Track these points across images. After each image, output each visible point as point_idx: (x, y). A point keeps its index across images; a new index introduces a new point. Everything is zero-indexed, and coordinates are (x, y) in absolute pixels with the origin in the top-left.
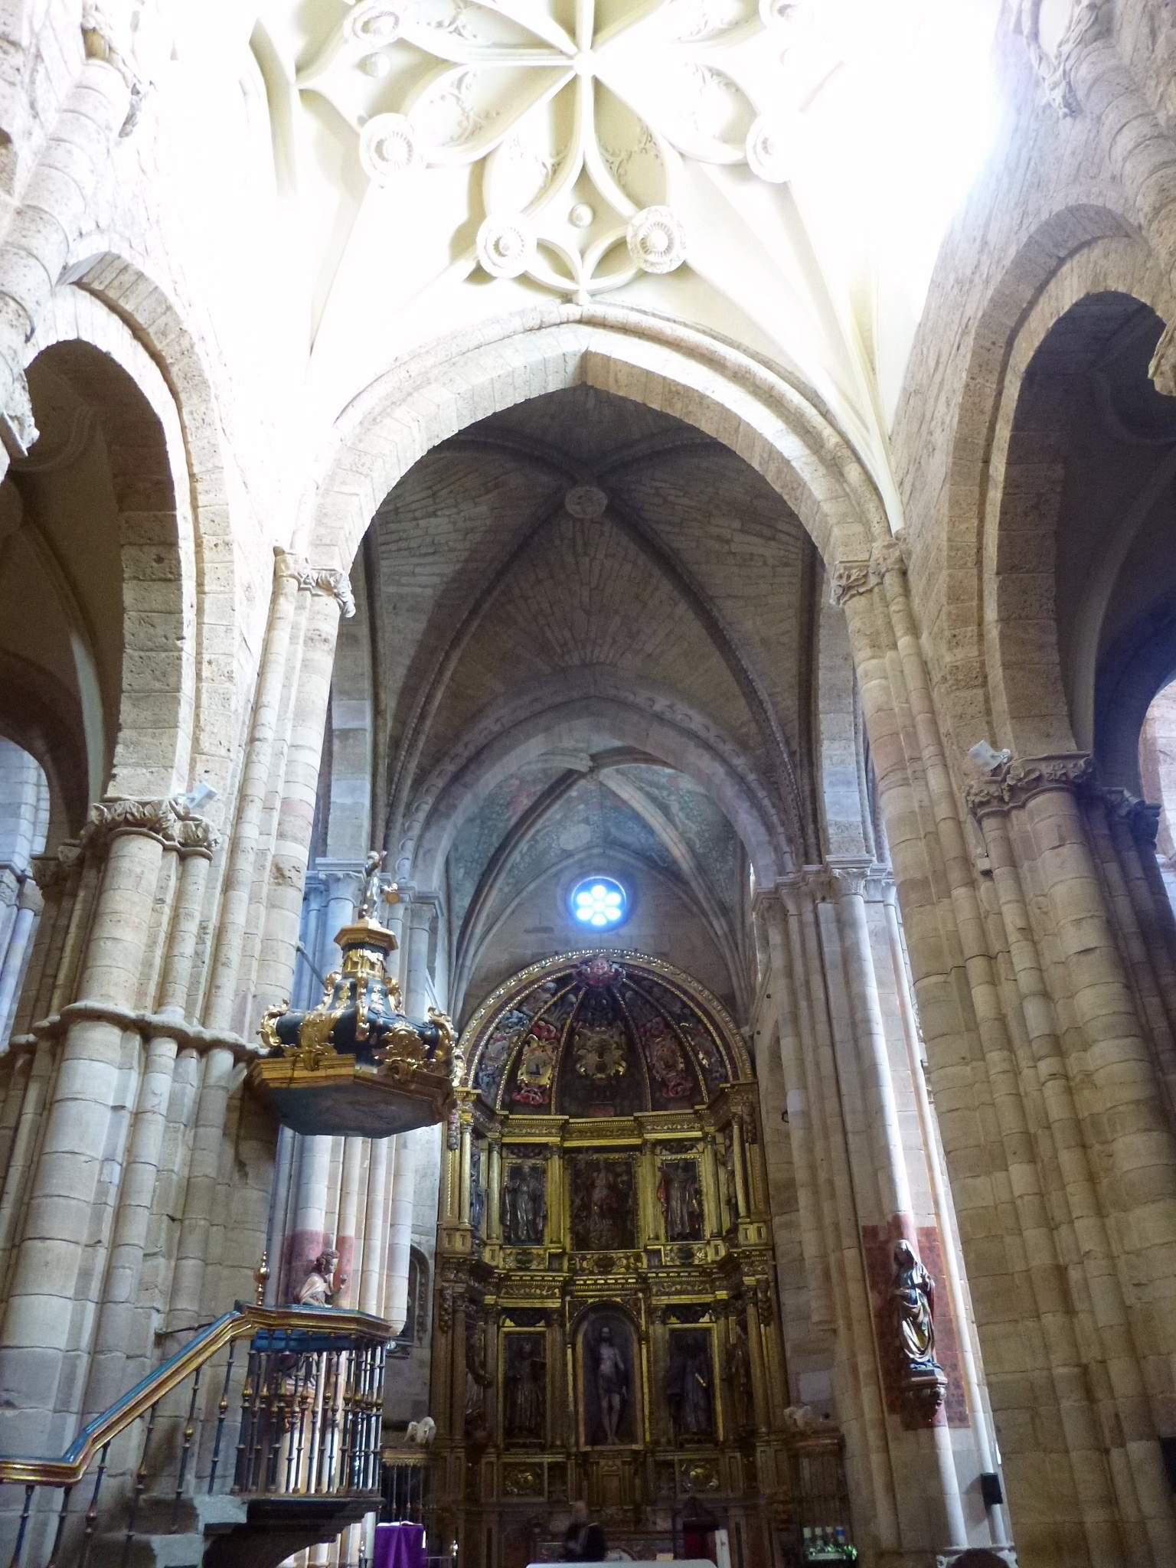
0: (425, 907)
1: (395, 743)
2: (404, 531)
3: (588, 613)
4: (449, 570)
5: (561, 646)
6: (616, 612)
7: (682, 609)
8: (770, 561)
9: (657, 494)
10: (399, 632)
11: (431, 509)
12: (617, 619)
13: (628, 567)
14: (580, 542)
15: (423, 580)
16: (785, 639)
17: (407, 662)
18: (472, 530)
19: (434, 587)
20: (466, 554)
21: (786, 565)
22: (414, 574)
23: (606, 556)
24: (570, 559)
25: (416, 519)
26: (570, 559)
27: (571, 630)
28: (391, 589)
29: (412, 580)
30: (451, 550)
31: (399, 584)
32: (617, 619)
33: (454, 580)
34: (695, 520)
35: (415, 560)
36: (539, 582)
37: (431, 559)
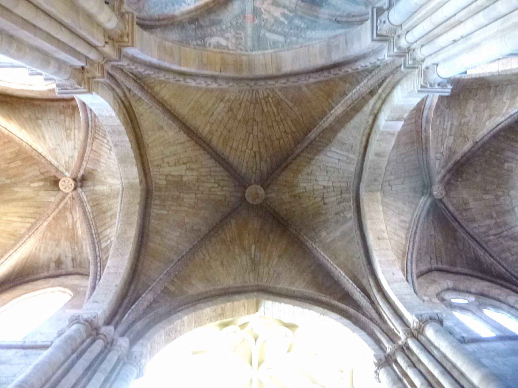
0: (384, 33)
1: (372, 93)
2: (339, 182)
3: (254, 120)
4: (321, 157)
5: (269, 102)
6: (240, 121)
7: (204, 130)
8: (166, 165)
10: (353, 136)
11: (325, 191)
12: (239, 117)
13: (234, 146)
14: (258, 159)
15: (336, 156)
16: (150, 133)
17: (352, 121)
19: (330, 150)
20: (313, 162)
21: (157, 166)
22: (339, 160)
23: (245, 151)
24: (263, 150)
25: (334, 187)
26: (263, 150)
28: (351, 156)
29: (341, 158)
31: (347, 157)
32: (239, 117)
34: (203, 176)
35: (338, 167)
36: (279, 140)
37: (330, 165)
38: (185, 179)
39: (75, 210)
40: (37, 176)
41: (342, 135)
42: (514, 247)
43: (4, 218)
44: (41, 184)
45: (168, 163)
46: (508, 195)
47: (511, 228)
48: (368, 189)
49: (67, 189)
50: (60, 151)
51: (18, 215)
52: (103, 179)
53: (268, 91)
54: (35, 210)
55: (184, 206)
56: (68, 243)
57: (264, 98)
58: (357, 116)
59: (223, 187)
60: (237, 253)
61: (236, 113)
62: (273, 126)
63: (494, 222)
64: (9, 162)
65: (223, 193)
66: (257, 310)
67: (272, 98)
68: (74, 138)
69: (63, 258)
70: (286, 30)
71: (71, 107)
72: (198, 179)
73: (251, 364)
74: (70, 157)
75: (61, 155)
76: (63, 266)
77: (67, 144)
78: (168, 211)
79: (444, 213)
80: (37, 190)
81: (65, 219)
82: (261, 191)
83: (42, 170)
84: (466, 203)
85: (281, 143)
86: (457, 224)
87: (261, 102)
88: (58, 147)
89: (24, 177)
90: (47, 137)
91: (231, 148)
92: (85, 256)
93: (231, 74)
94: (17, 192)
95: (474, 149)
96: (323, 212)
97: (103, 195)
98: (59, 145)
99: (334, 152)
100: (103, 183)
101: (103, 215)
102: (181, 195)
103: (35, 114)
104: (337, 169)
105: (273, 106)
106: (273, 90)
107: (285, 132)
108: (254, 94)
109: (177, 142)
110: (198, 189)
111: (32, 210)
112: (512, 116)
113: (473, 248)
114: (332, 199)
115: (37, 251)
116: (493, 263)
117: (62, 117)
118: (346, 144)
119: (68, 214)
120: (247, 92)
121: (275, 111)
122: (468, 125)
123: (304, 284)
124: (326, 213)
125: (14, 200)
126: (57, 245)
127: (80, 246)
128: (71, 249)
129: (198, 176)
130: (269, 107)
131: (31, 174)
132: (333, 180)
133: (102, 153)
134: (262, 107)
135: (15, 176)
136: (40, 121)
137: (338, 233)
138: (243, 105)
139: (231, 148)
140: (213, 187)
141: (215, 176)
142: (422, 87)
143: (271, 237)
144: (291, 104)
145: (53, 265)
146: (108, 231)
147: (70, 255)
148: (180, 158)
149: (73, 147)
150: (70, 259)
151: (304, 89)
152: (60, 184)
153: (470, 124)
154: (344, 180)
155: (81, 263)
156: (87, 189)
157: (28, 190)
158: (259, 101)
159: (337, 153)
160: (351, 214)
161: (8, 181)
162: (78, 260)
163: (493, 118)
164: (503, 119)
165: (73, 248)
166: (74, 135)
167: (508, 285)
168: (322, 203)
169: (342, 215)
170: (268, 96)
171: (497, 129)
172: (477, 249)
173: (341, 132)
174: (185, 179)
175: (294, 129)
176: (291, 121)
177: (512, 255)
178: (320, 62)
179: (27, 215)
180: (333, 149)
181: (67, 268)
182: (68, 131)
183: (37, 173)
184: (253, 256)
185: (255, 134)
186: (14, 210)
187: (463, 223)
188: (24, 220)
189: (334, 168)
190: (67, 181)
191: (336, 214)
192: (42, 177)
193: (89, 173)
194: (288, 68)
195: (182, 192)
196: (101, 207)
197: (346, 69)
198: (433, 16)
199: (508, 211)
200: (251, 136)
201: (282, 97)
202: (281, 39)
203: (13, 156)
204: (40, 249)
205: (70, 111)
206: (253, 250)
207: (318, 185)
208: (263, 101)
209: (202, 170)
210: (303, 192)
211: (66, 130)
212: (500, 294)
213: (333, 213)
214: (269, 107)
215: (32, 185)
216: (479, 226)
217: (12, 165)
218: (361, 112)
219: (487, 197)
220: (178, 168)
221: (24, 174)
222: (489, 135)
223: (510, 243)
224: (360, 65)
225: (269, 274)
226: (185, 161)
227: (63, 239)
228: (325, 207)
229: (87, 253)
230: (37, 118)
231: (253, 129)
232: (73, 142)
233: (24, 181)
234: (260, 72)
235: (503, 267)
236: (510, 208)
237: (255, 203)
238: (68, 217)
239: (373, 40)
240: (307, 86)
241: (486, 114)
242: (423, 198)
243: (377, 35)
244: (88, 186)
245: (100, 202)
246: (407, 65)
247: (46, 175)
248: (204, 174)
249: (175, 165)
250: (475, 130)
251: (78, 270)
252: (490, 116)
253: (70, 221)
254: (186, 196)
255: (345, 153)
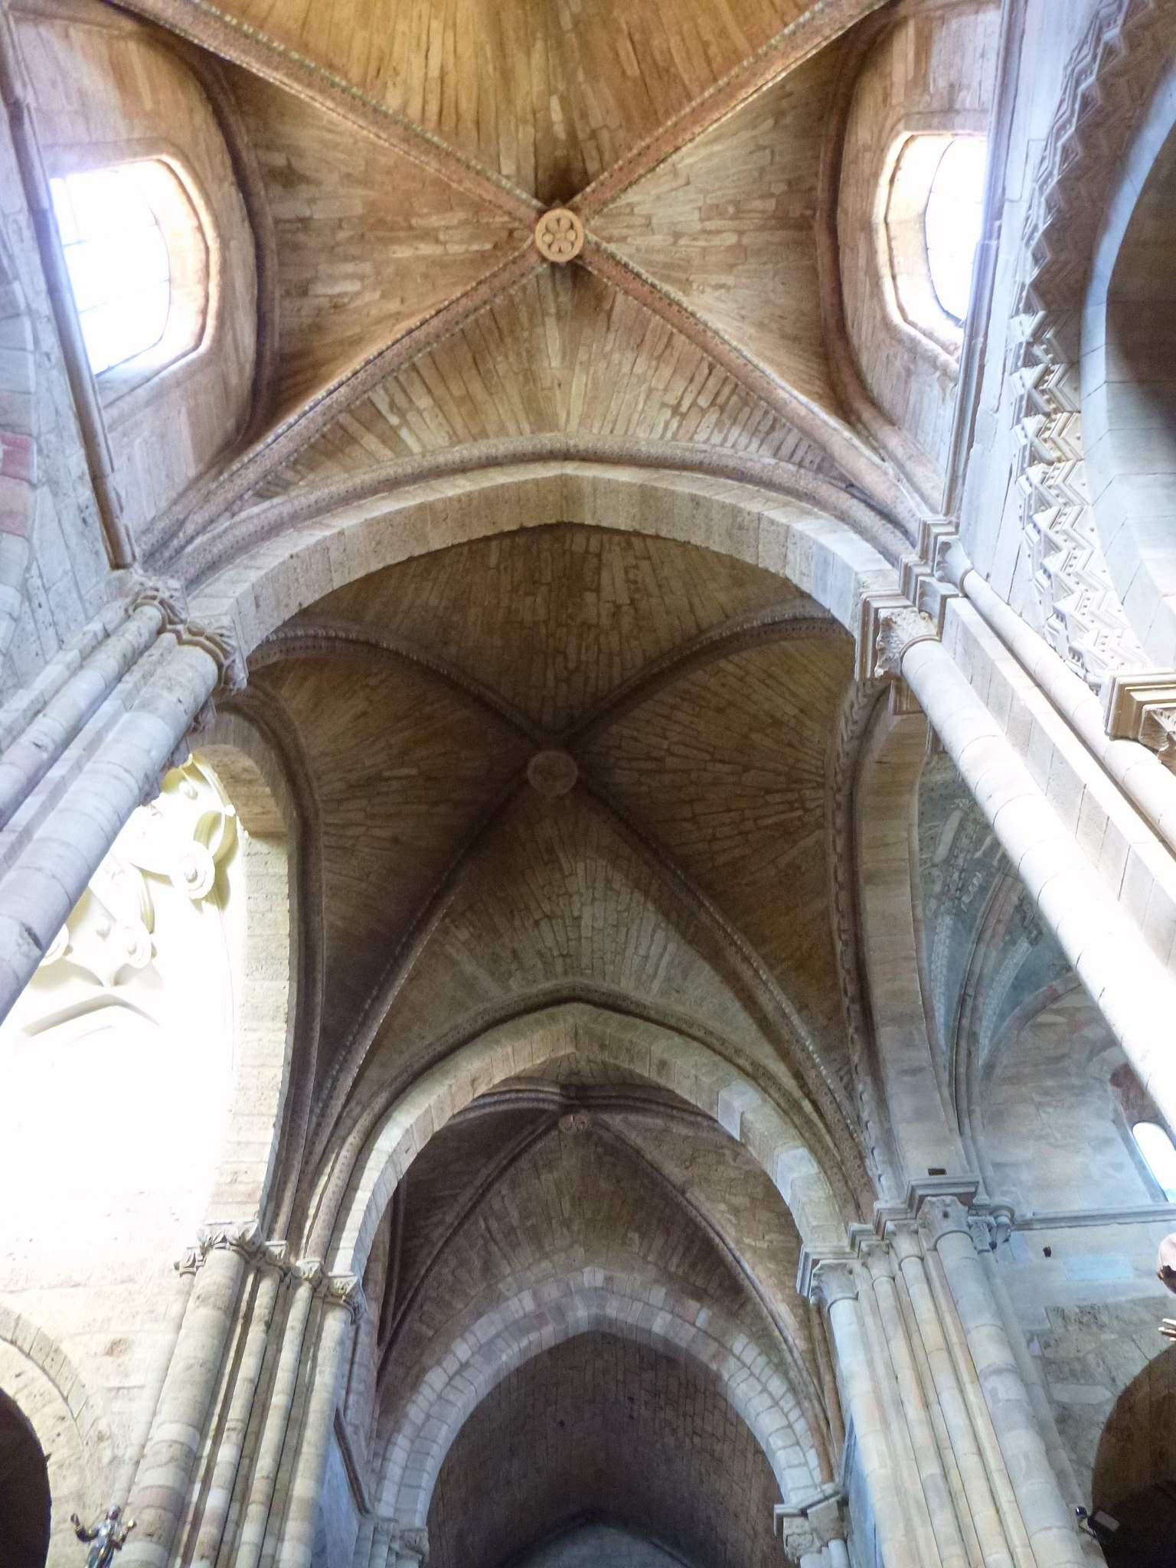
0: (926, 1208)
3: (747, 769)
4: (651, 916)
5: (792, 810)
6: (745, 736)
9: (568, 681)
10: (703, 999)
12: (755, 737)
13: (679, 715)
15: (655, 950)
17: (738, 1005)
18: (608, 881)
19: (668, 940)
20: (638, 896)
22: (646, 957)
23: (666, 738)
25: (580, 938)
27: (768, 791)
28: (656, 985)
29: (652, 960)
30: (628, 910)
32: (755, 737)
33: (666, 915)
34: (597, 639)
35: (629, 952)
36: (694, 819)
37: (634, 933)
38: (590, 597)
39: (473, 238)
40: (584, 115)
41: (705, 975)
42: (470, 1272)
43: (436, 25)
44: (560, 131)
45: (636, 567)
46: (574, 1242)
47: (505, 1256)
48: (581, 1032)
49: (548, 238)
50: (668, 187)
51: (450, 67)
52: (583, 355)
53: (819, 812)
54: (469, 117)
55: (511, 599)
56: (359, 210)
57: (802, 801)
58: (750, 1021)
59: (568, 681)
60: (393, 741)
61: (768, 731)
62: (729, 810)
63: (515, 1223)
64: (637, 37)
65: (551, 683)
66: (254, 834)
67: (800, 818)
68: (710, 232)
69: (304, 191)
70: (960, 861)
71: (809, 212)
72: (589, 627)
73: (153, 947)
74: (649, 218)
75: (653, 192)
76: (277, 190)
77: (688, 207)
78: (497, 568)
79: (525, 1132)
80: (537, 116)
81: (445, 205)
82: (562, 787)
83: (605, 136)
84: (550, 1166)
85: (688, 826)
86: (505, 1162)
87: (791, 790)
88: (682, 181)
89: (581, 76)
90: (717, 148)
91: (674, 707)
92: (324, 268)
93: (869, 775)
94: (529, 55)
95: (670, 1187)
96: (517, 923)
97: (531, 358)
98: (688, 183)
99: (665, 949)
100: (569, 354)
101: (470, 359)
102: (544, 589)
103: (795, 108)
104: (624, 950)
105: (783, 817)
106: (820, 826)
107: (714, 839)
108: (812, 777)
109: (696, 600)
110: (559, 625)
111: (467, 106)
112: (738, 1262)
113: (455, 1197)
114: (549, 937)
115: (325, 122)
116: (433, 1245)
117: (782, 187)
118: (685, 978)
119: (460, 215)
120: (819, 764)
121: (770, 821)
122: (719, 1163)
123: (339, 923)
124: (515, 930)
125: (501, 46)
126: (348, 175)
127: (353, 250)
128: (340, 220)
129: (597, 626)
130: (781, 808)
131: (592, 100)
132: (595, 938)
133: (666, 372)
134: (777, 792)
135: (585, 46)
136: (770, 122)
137: (469, 968)
138: (787, 750)
139: (674, 707)
140: (566, 659)
141: (597, 662)
142: (816, 1262)
143: (443, 809)
144: (783, 862)
145: (279, 160)
146: (424, 402)
147: (319, 213)
148: (649, 595)
149: (679, 228)
150: (308, 213)
151: (818, 905)
152: (560, 214)
153: (721, 1168)
154: (597, 963)
155: (296, 247)
156: (547, 285)
157: (535, 89)
158: (794, 786)
159: (662, 955)
160: (518, 989)
161: (566, 21)
162: (302, 237)
163: (732, 1218)
164: (732, 1245)
165: (345, 225)
166: (719, 232)
167: (395, 1284)
168: (537, 915)
169: (513, 967)
170: (806, 810)
171: (713, 1235)
172: (457, 1208)
173: (712, 973)
174: (590, 597)
175: (721, 860)
176: (743, 858)
177: (453, 1273)
178: (880, 992)
179: (450, 92)
180: (672, 947)
181: (270, 203)
182: (731, 210)
183: (597, 118)
184: (386, 774)
185: (710, 766)
186: (466, 50)
187: (507, 1176)
188: (435, 86)
189: (626, 943)
190: (571, 235)
191: (514, 952)
192: (581, 135)
193: (600, 298)
194: (873, 901)
195: (550, 591)
196: (492, 347)
197: (858, 1047)
198: (944, 1354)
199: (540, 1247)
200: (707, 757)
201: (802, 844)
202: (942, 851)
203: (658, 56)
204: (331, 131)
205: (796, 210)
206: (405, 771)
207: (583, 905)
208: (795, 796)
209: (614, 639)
210: (561, 869)
211: (737, 203)
212: (376, 1283)
213: (516, 945)
214: (781, 808)
215: (555, 103)
216: (503, 1198)
217: (625, 48)
218: (760, 1034)
219: (567, 1206)
220: (620, 582)
221: (592, 76)
222: (699, 1219)
223: (477, 1263)
224: (864, 1086)
225: (345, 826)
226: (643, 605)
227: (372, 194)
228: (529, 923)
229: (333, 279)
230: (779, 115)
231: (723, 762)
232: (698, 226)
233: (570, 79)
234: (868, 831)
235: (429, 1270)
236: (547, 1248)
237: (530, 772)
238: (448, 215)
239: (913, 1189)
240: (824, 915)
241: (741, 1201)
242: (556, 1090)
243: (922, 1198)
244: (557, 295)
245: (508, 340)
246: (858, 1239)
247: (590, 147)
248: (602, 640)
249: (628, 581)
250: (707, 1180)
251: (271, 243)
252: (736, 1211)
253: (435, 221)
254: (539, 600)
255: (662, 973)
